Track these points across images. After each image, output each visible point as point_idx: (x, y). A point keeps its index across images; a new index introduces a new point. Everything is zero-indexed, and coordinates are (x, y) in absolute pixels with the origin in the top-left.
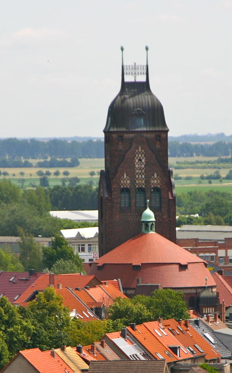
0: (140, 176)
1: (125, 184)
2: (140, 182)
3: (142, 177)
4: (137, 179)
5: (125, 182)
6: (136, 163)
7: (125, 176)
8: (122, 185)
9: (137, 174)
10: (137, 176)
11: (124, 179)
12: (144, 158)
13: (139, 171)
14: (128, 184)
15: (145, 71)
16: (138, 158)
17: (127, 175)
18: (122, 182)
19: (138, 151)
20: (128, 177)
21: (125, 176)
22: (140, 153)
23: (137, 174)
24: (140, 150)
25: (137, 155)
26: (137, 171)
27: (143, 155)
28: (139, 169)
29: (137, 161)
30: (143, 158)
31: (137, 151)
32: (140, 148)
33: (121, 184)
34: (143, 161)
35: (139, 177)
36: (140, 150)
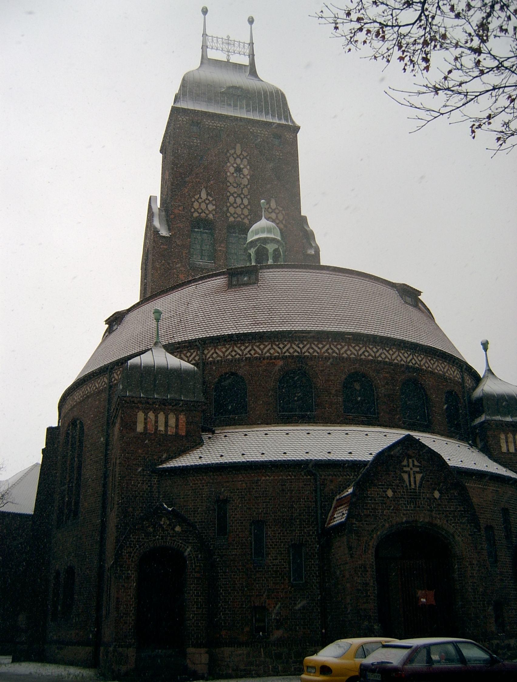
0: (239, 201)
1: (203, 211)
2: (239, 211)
3: (242, 203)
4: (232, 205)
5: (203, 206)
6: (228, 174)
7: (204, 195)
8: (196, 210)
9: (232, 195)
10: (231, 199)
11: (200, 201)
12: (248, 167)
13: (236, 190)
14: (210, 212)
15: (247, 51)
16: (235, 165)
17: (207, 195)
18: (196, 205)
19: (235, 153)
20: (211, 199)
21: (204, 195)
22: (238, 156)
23: (232, 195)
24: (238, 152)
25: (231, 160)
26: (232, 190)
27: (245, 162)
28: (235, 185)
29: (232, 170)
30: (245, 167)
31: (232, 151)
32: (238, 146)
33: (193, 210)
34: (246, 172)
35: (235, 202)
36: (238, 152)
